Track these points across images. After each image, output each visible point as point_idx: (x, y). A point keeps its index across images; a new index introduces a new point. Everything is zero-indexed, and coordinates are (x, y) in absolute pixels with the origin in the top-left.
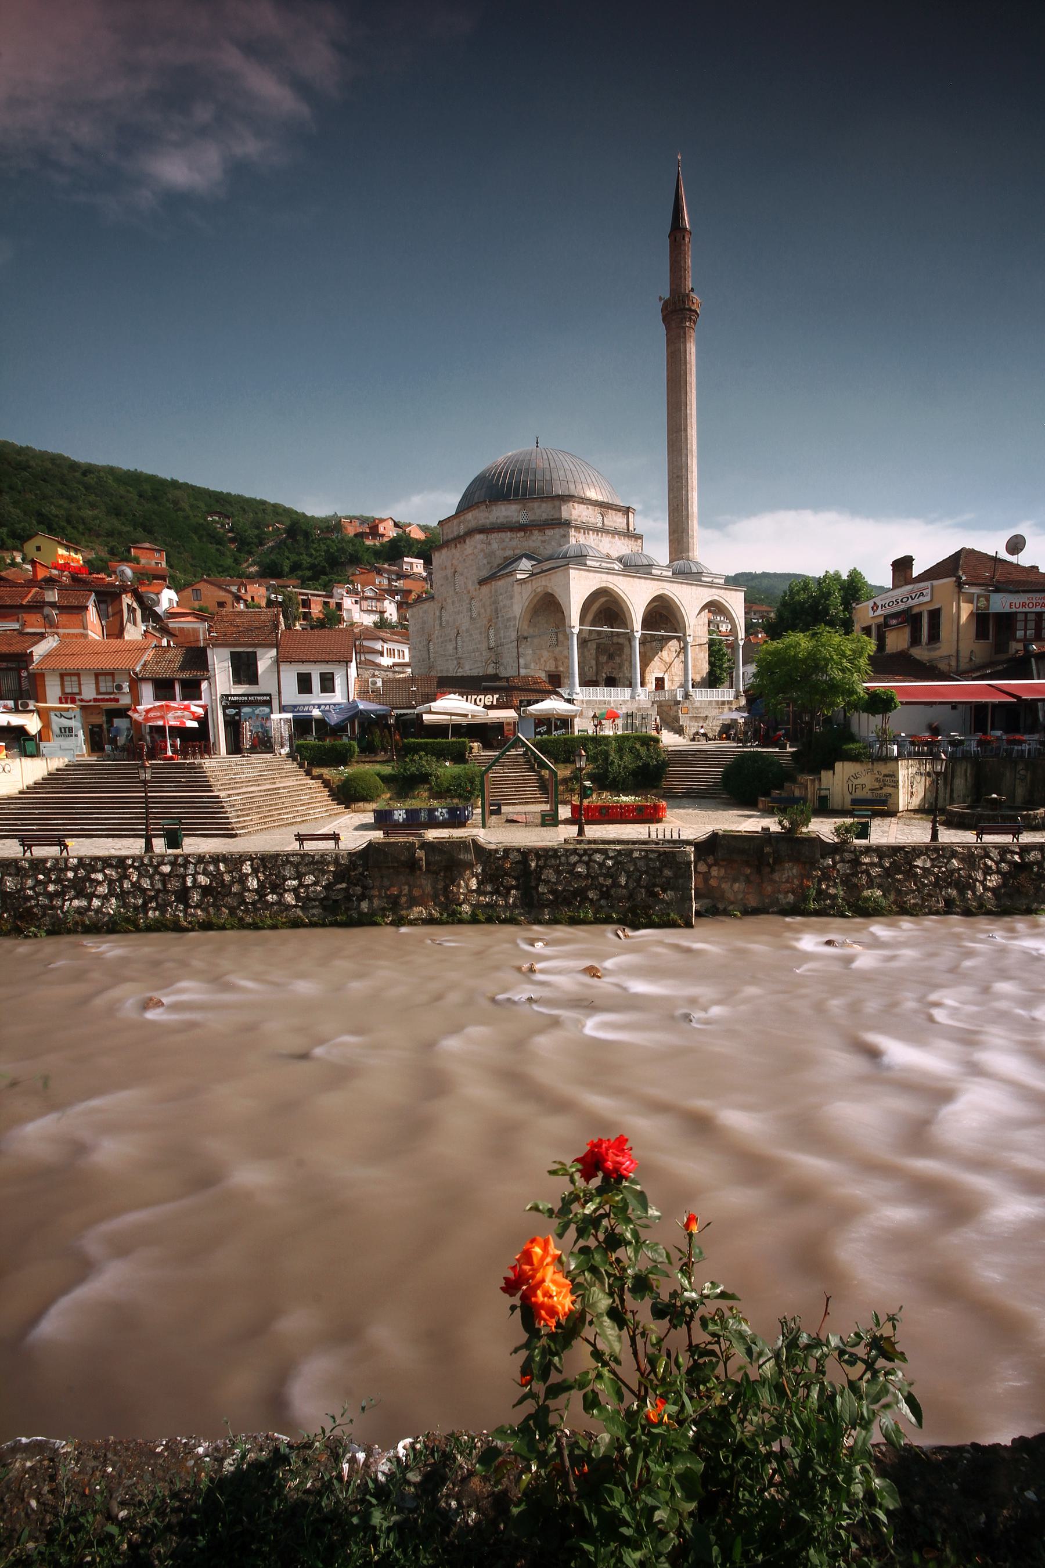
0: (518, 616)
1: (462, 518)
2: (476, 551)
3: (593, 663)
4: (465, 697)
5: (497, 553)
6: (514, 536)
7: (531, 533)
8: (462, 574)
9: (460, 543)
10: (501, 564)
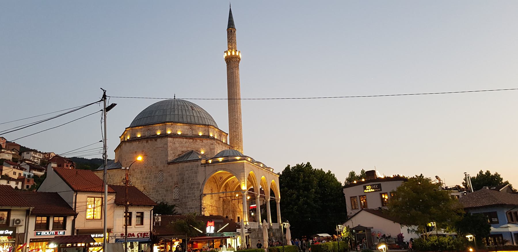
0: (201, 183)
1: (150, 128)
2: (165, 146)
5: (178, 148)
6: (188, 141)
7: (196, 141)
8: (152, 157)
9: (150, 140)
10: (181, 155)
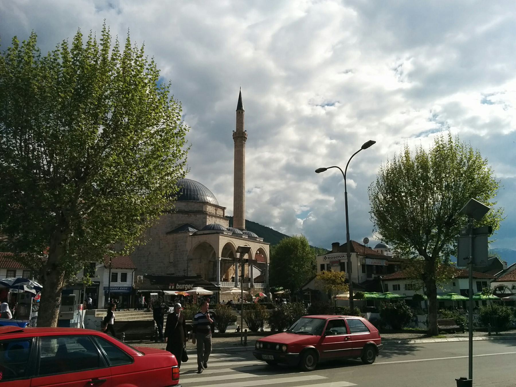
3: (212, 270)
4: (180, 285)
6: (183, 216)
10: (176, 227)
